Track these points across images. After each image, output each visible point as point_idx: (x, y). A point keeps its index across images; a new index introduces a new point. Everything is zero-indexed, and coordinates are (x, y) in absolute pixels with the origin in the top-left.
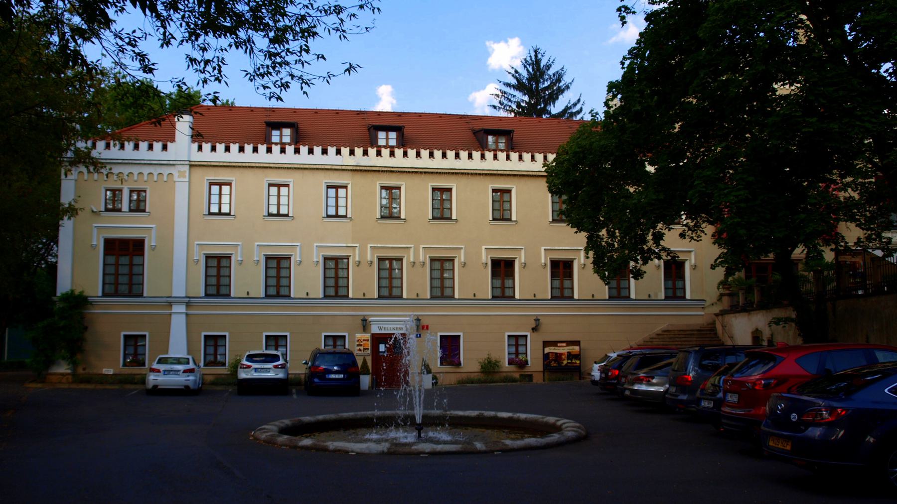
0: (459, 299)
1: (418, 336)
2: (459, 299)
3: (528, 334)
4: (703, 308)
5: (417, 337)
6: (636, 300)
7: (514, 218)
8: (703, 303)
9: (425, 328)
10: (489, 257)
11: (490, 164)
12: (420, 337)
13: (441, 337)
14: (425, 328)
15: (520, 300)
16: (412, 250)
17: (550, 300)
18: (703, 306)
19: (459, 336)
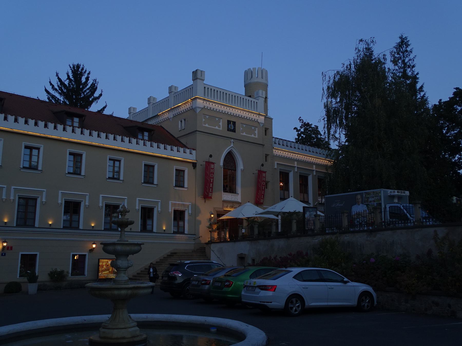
0: (38, 228)
1: (4, 254)
2: (38, 228)
3: (87, 254)
4: (194, 239)
5: (2, 255)
6: (156, 233)
7: (83, 173)
8: (194, 236)
9: (10, 249)
10: (63, 198)
11: (67, 136)
12: (5, 255)
13: (22, 255)
14: (10, 249)
15: (83, 230)
16: (4, 190)
17: (103, 231)
18: (194, 238)
19: (36, 255)
